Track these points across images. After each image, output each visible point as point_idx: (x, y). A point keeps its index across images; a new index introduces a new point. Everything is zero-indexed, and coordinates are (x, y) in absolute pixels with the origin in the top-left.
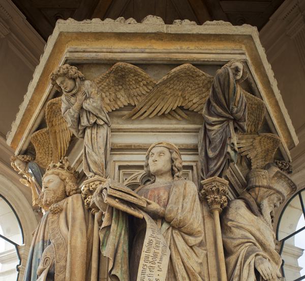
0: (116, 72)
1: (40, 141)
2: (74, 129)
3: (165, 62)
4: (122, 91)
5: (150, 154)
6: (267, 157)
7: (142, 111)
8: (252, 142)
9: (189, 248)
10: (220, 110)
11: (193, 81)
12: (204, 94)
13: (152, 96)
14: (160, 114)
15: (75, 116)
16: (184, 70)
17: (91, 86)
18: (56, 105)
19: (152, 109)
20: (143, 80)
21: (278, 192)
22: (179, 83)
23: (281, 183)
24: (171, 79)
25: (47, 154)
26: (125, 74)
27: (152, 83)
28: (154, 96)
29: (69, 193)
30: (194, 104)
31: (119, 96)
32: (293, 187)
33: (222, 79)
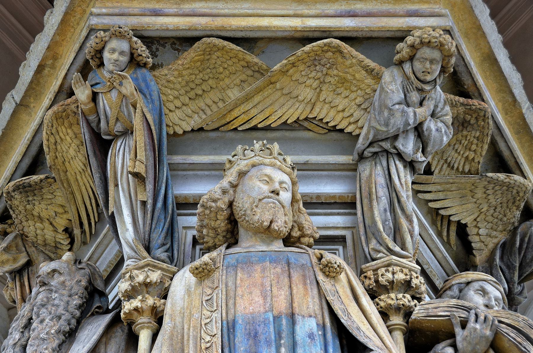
0: (470, 110)
1: (208, 60)
2: (374, 136)
3: (506, 153)
5: (476, 285)
10: (516, 278)
11: (507, 207)
12: (495, 233)
13: (463, 181)
14: (442, 212)
17: (445, 101)
18: (338, 54)
19: (441, 195)
24: (502, 184)
25: (188, 89)
26: (473, 125)
27: (476, 165)
29: (303, 236)
30: (478, 234)
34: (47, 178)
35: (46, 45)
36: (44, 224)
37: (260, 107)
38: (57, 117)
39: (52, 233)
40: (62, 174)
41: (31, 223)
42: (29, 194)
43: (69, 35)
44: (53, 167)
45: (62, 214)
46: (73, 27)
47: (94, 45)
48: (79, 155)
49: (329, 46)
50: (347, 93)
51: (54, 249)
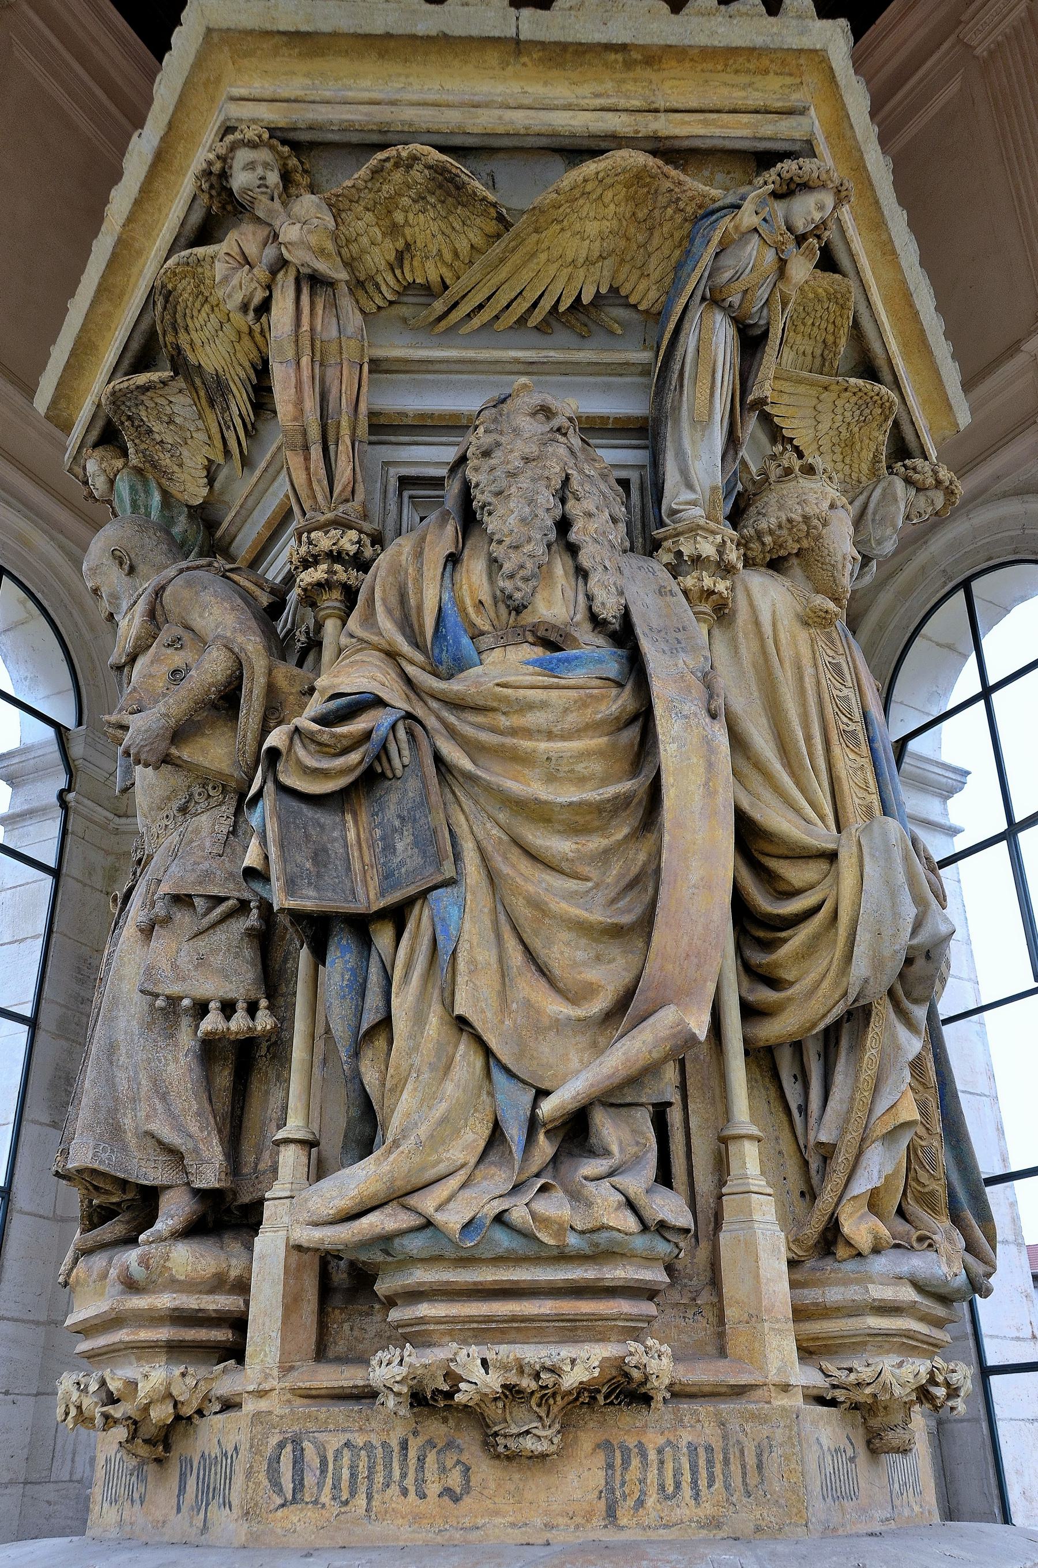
34: (494, 205)
35: (672, 40)
36: (387, 240)
37: (791, 400)
38: (639, 177)
39: (383, 262)
40: (531, 229)
41: (369, 217)
42: (438, 192)
43: (710, 66)
44: (537, 212)
45: (444, 262)
46: (726, 65)
47: (815, 175)
48: (597, 244)
49: (890, 407)
50: (838, 457)
51: (354, 282)
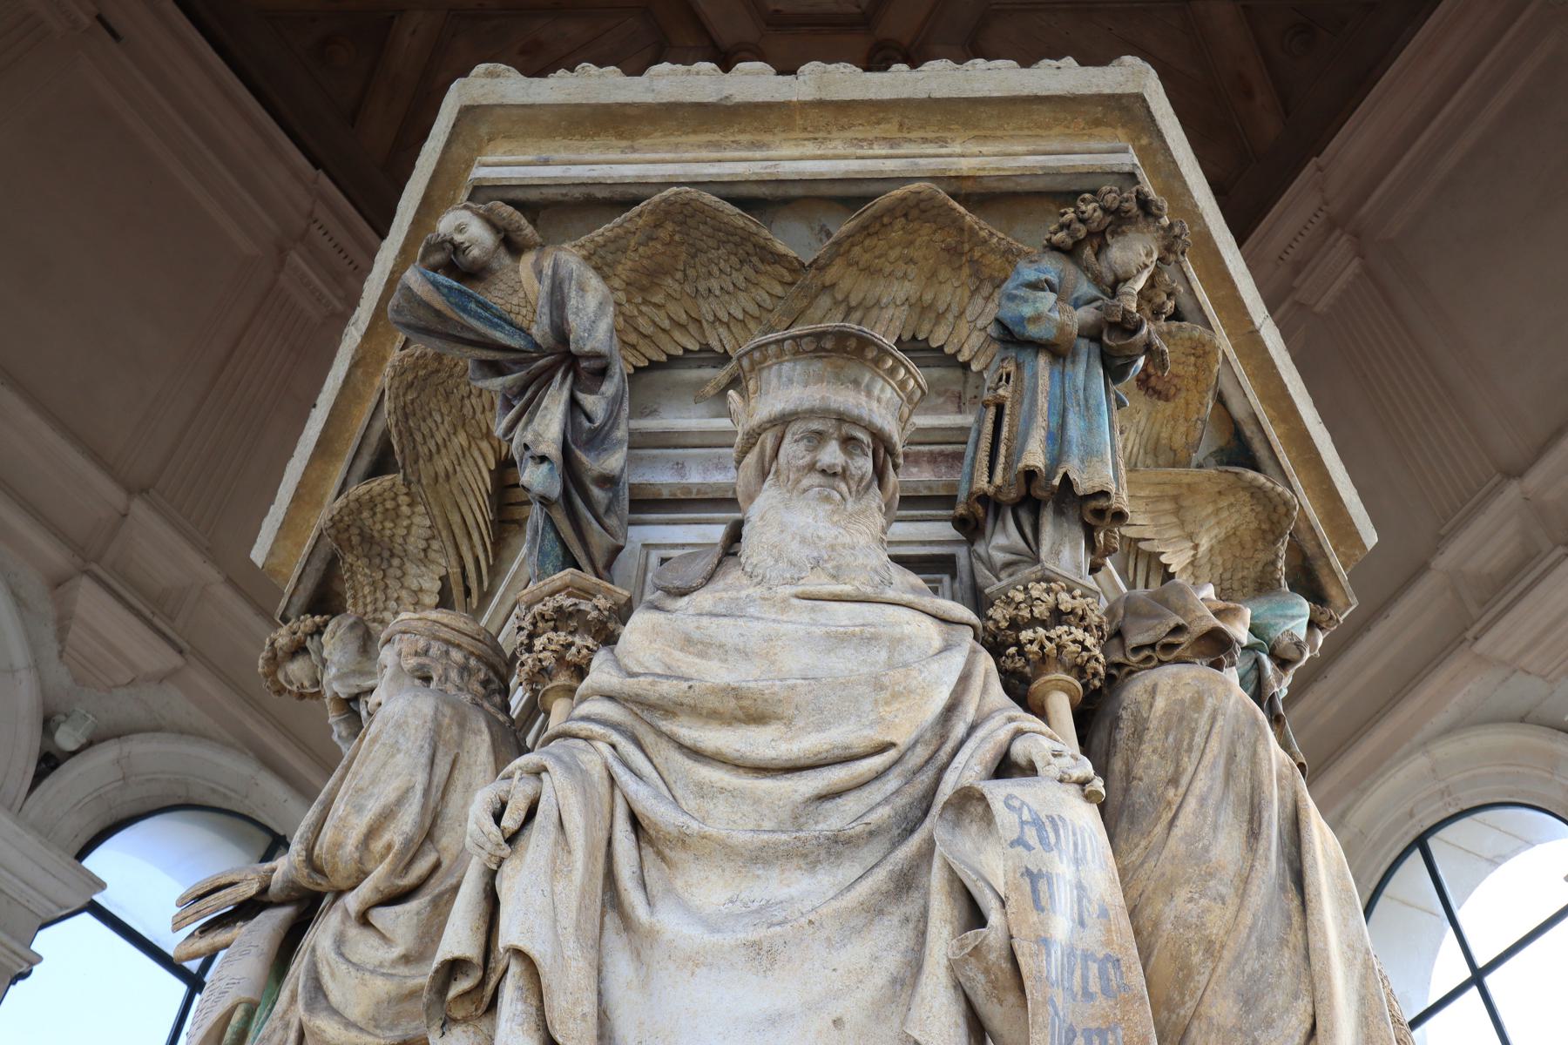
4: (408, 565)
6: (987, 272)
7: (470, 567)
8: (836, 303)
9: (354, 932)
11: (451, 376)
13: (436, 511)
15: (344, 734)
16: (396, 384)
19: (476, 536)
20: (394, 499)
21: (782, 422)
22: (429, 421)
23: (774, 382)
28: (442, 506)
31: (415, 586)
32: (829, 345)
33: (409, 319)
